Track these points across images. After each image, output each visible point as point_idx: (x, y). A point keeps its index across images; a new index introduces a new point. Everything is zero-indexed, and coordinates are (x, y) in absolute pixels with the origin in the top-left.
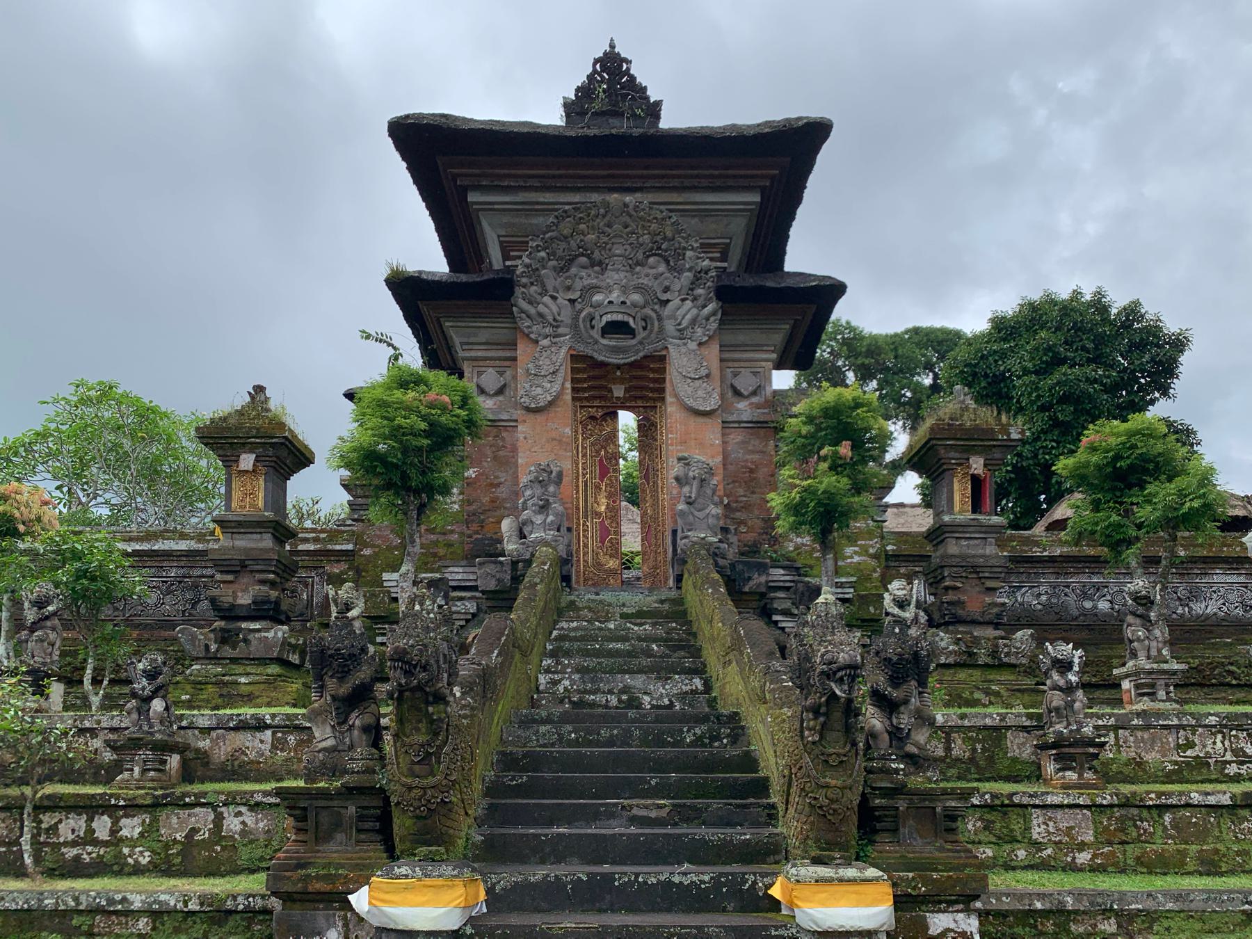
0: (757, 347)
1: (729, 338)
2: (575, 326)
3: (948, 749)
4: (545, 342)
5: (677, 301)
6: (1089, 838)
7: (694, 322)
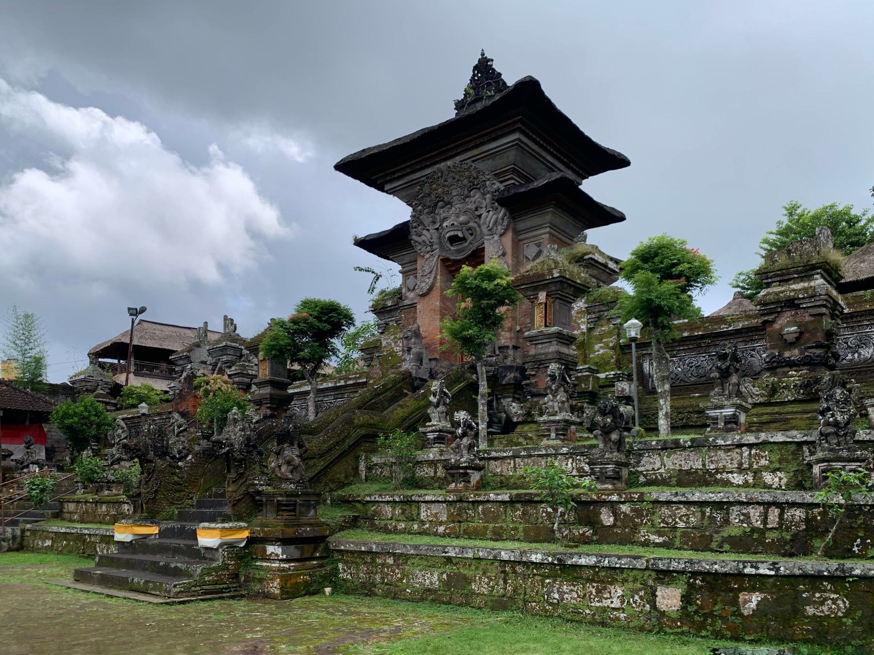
0: (539, 227)
1: (521, 226)
2: (440, 243)
3: (436, 472)
4: (427, 256)
5: (485, 214)
6: (444, 519)
7: (496, 222)
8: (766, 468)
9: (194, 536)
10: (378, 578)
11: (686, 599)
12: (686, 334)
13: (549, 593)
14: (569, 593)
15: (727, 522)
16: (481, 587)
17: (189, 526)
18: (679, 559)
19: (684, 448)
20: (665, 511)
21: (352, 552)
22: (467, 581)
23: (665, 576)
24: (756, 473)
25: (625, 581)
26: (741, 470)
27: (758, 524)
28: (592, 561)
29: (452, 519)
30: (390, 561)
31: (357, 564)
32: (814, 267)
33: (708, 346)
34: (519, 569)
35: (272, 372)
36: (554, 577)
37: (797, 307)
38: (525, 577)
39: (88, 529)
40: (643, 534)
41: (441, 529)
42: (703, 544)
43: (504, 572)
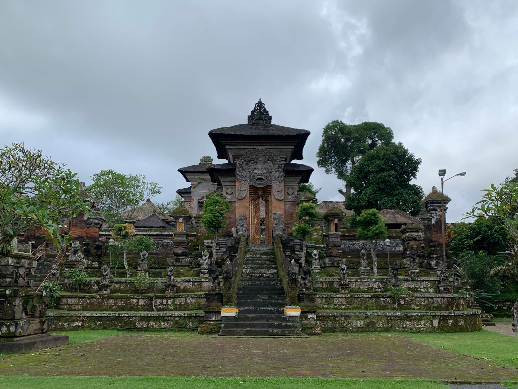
0: (293, 182)
1: (287, 180)
2: (250, 178)
3: (322, 286)
4: (243, 182)
5: (274, 172)
6: (345, 303)
7: (278, 177)
8: (429, 287)
9: (283, 313)
10: (337, 325)
11: (439, 323)
12: (347, 235)
13: (402, 325)
14: (409, 324)
15: (434, 302)
16: (379, 325)
17: (281, 309)
18: (437, 313)
19: (409, 281)
20: (418, 299)
21: (324, 316)
22: (374, 323)
23: (434, 317)
24: (427, 288)
25: (424, 319)
26: (424, 288)
27: (440, 303)
28: (416, 314)
29: (348, 303)
30: (343, 319)
31: (327, 321)
32: (420, 230)
33: (353, 239)
34: (392, 318)
35: (186, 229)
36: (404, 319)
37: (416, 240)
38: (394, 320)
39: (127, 314)
40: (413, 306)
41: (343, 307)
42: (429, 309)
43: (387, 319)
